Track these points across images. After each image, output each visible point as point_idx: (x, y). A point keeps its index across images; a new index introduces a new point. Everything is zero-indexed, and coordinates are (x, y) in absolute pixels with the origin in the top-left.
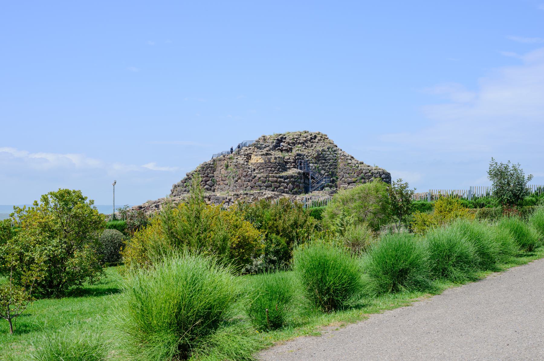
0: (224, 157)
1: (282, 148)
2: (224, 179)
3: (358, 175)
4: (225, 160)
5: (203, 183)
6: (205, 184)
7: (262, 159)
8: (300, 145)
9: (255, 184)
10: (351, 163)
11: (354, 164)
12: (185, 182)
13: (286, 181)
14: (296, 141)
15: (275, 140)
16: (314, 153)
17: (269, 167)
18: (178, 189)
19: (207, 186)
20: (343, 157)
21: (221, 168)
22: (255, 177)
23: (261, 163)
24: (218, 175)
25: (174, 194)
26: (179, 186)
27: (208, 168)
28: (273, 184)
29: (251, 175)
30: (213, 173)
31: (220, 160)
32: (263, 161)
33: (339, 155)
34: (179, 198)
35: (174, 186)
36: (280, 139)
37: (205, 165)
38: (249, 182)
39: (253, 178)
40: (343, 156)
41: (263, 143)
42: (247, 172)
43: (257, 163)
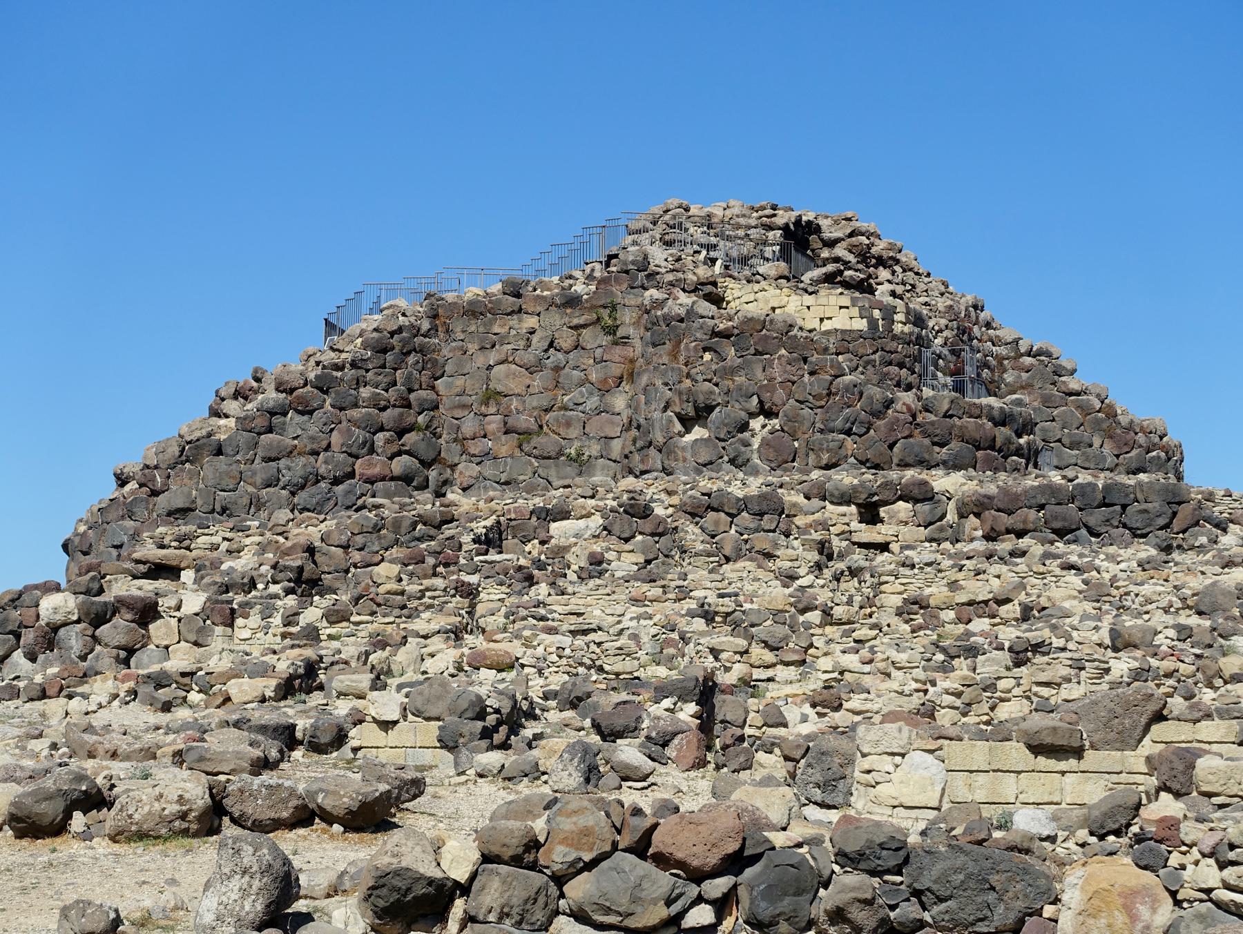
0: (518, 296)
1: (841, 273)
2: (525, 421)
3: (1117, 456)
4: (520, 310)
5: (388, 441)
6: (395, 449)
7: (855, 311)
8: (884, 274)
9: (891, 447)
10: (1078, 394)
11: (1098, 396)
12: (270, 430)
13: (1022, 441)
14: (869, 247)
15: (770, 228)
16: (943, 322)
17: (890, 364)
18: (211, 467)
19: (400, 464)
20: (1028, 360)
21: (493, 357)
22: (888, 404)
23: (846, 339)
24: (468, 400)
25: (173, 498)
26: (219, 452)
27: (409, 353)
28: (980, 454)
29: (861, 394)
30: (433, 388)
31: (473, 311)
32: (862, 325)
33: (1002, 350)
34: (593, 497)
35: (175, 450)
36: (792, 227)
37: (392, 334)
38: (848, 433)
39: (878, 414)
40: (1029, 354)
41: (713, 240)
42: (836, 377)
43: (827, 333)
